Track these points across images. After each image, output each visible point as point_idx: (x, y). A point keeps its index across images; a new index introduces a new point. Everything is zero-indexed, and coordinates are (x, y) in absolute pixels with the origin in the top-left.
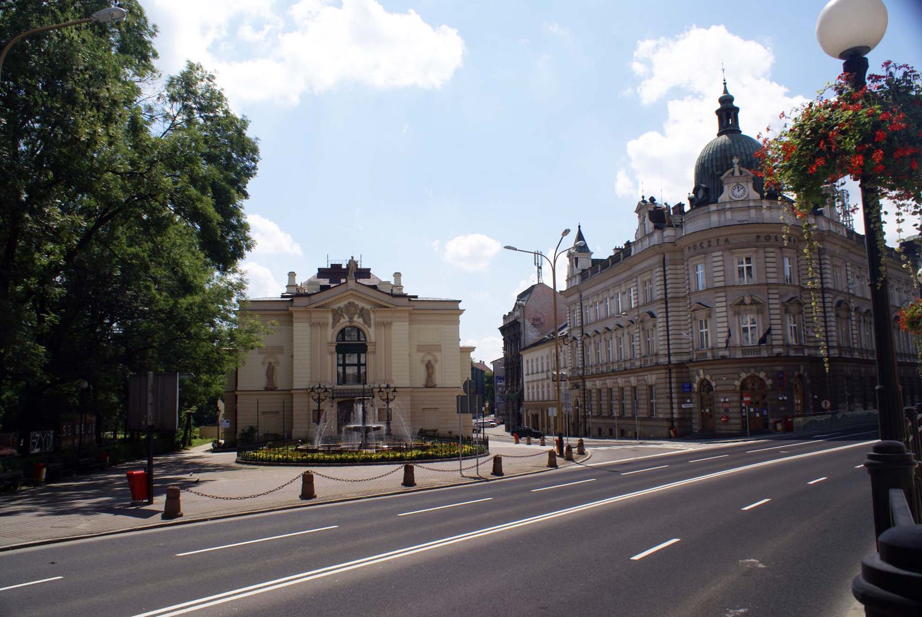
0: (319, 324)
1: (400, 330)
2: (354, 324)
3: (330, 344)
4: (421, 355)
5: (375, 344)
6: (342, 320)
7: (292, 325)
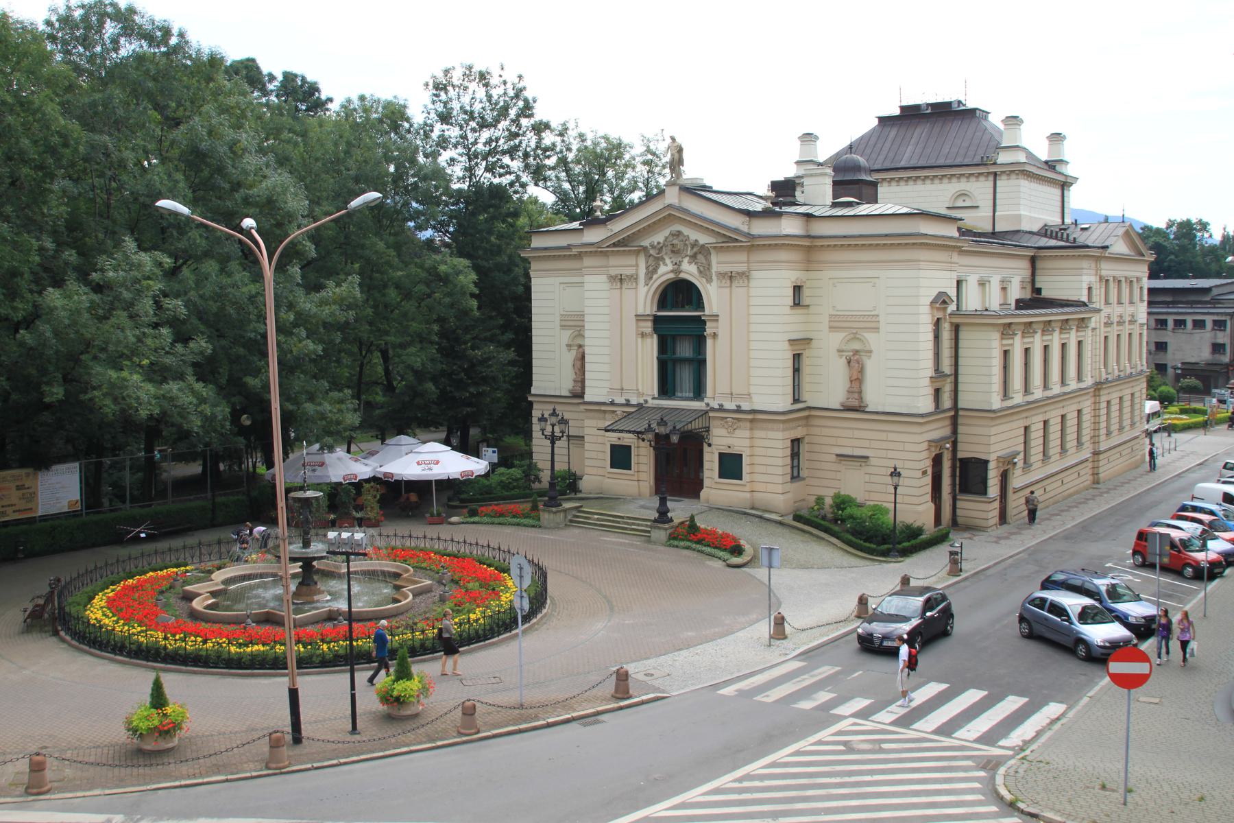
2: (682, 276)
3: (639, 318)
5: (715, 318)
6: (663, 269)
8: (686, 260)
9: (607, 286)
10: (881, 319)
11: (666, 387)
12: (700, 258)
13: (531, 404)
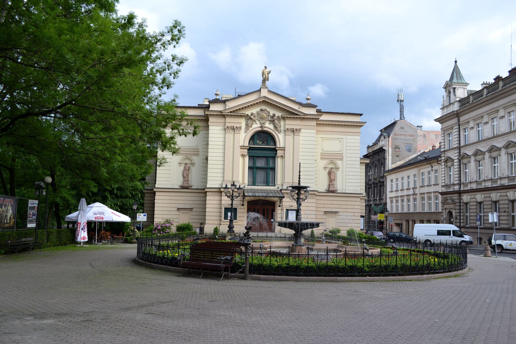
3: (242, 147)
4: (324, 163)
5: (283, 149)
6: (254, 126)
8: (267, 123)
9: (223, 132)
10: (344, 155)
13: (155, 192)
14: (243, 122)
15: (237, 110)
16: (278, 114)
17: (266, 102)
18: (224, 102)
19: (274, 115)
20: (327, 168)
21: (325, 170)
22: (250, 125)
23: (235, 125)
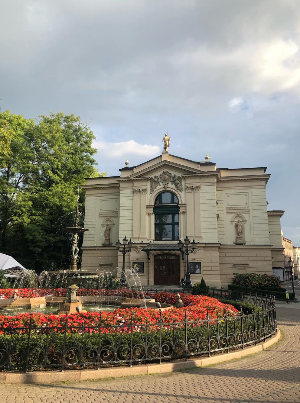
0: (139, 191)
1: (208, 191)
2: (168, 189)
3: (148, 207)
5: (185, 206)
6: (159, 187)
7: (119, 193)
8: (170, 183)
9: (131, 195)
11: (158, 237)
12: (177, 181)
14: (148, 185)
15: (142, 175)
16: (179, 174)
17: (166, 165)
18: (132, 169)
19: (175, 176)
20: (233, 221)
21: (232, 224)
22: (154, 187)
23: (141, 188)
